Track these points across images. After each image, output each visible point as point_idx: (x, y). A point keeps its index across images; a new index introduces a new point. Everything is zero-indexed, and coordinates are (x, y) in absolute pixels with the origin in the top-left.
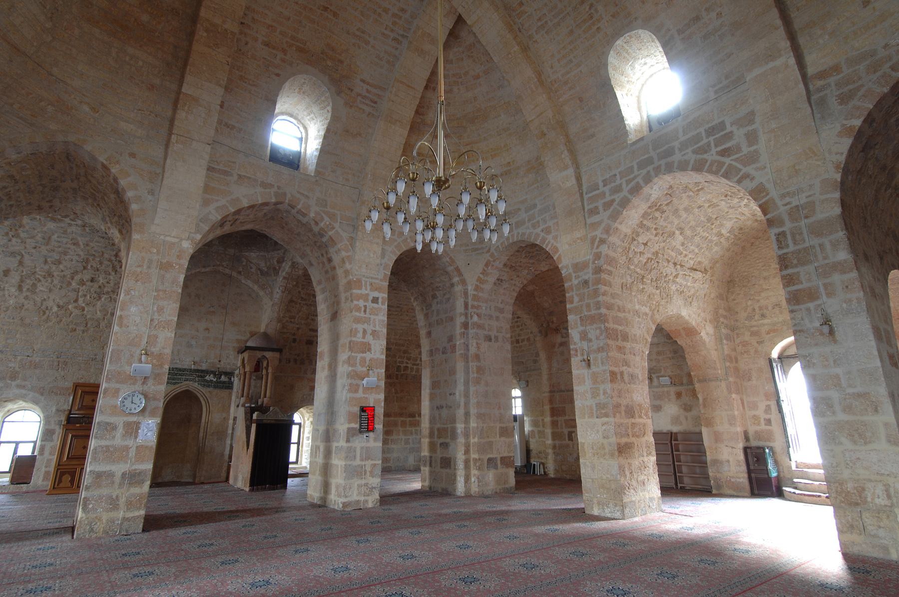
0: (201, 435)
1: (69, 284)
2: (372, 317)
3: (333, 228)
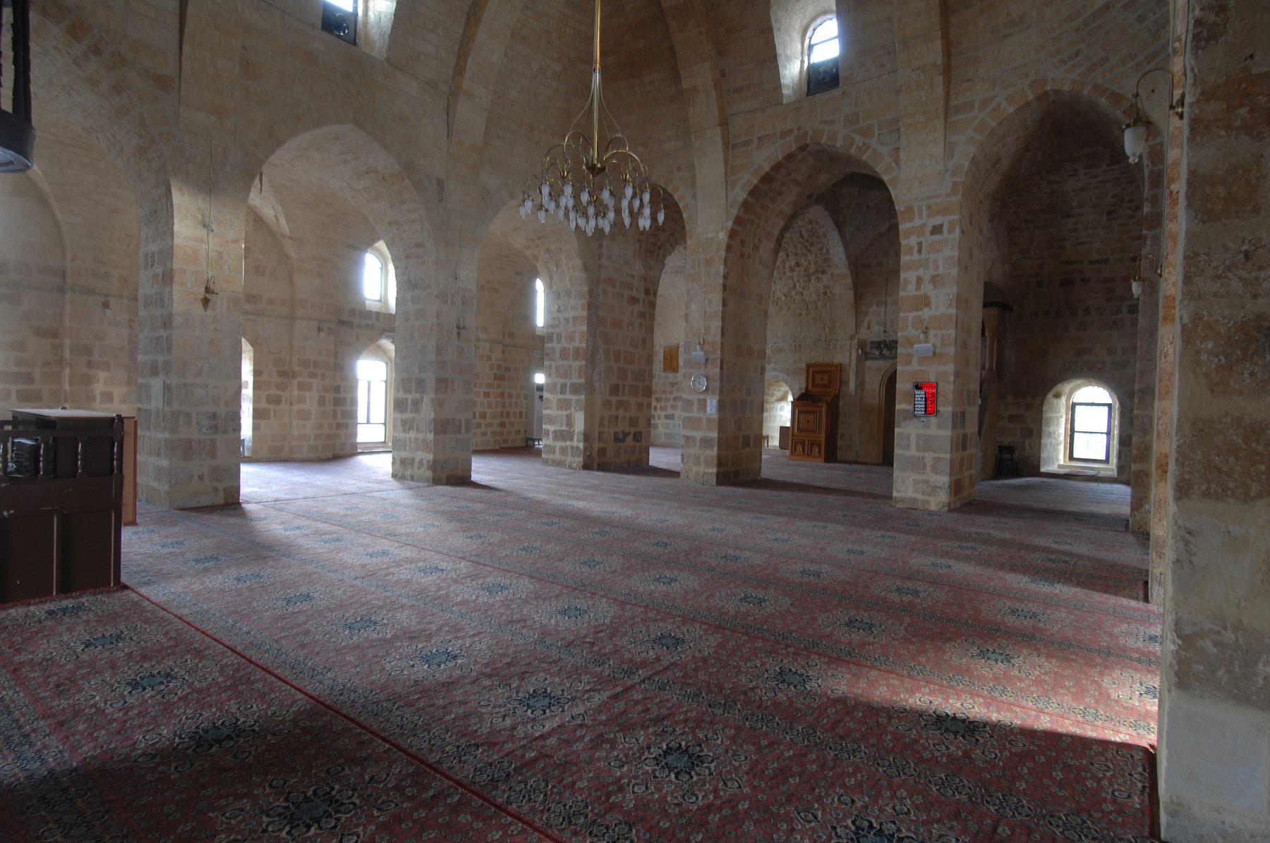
1: (784, 273)
2: (932, 256)
3: (868, 148)
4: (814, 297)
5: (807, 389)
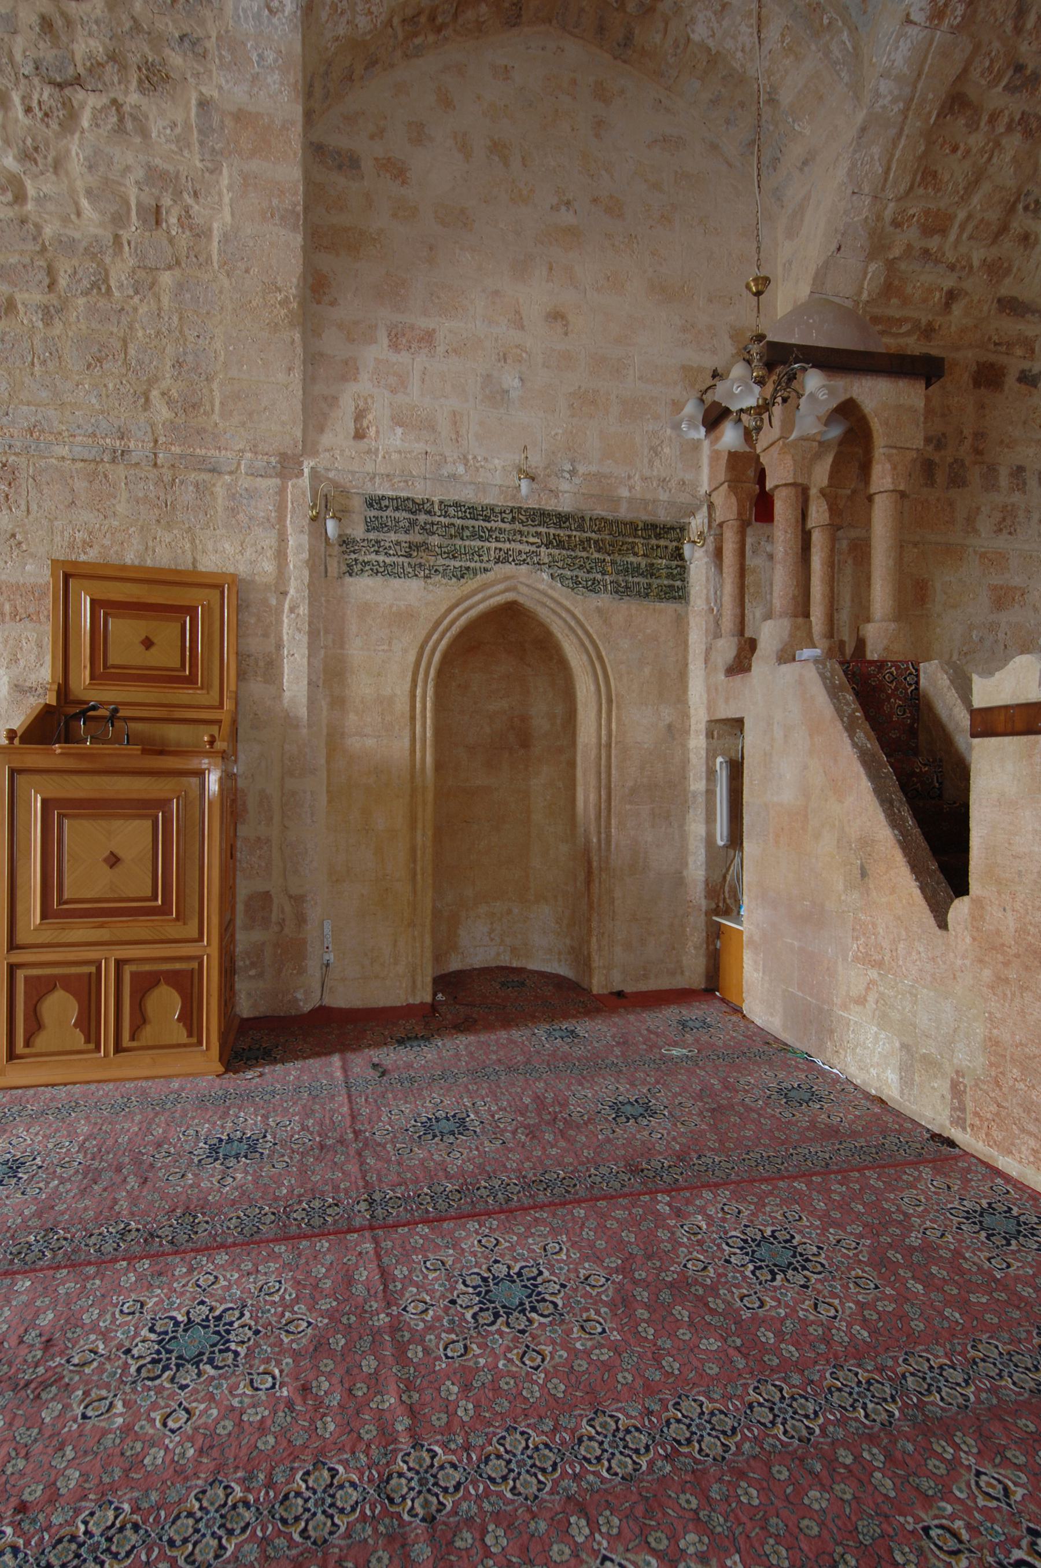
0: (586, 796)
4: (92, 220)
5: (63, 690)
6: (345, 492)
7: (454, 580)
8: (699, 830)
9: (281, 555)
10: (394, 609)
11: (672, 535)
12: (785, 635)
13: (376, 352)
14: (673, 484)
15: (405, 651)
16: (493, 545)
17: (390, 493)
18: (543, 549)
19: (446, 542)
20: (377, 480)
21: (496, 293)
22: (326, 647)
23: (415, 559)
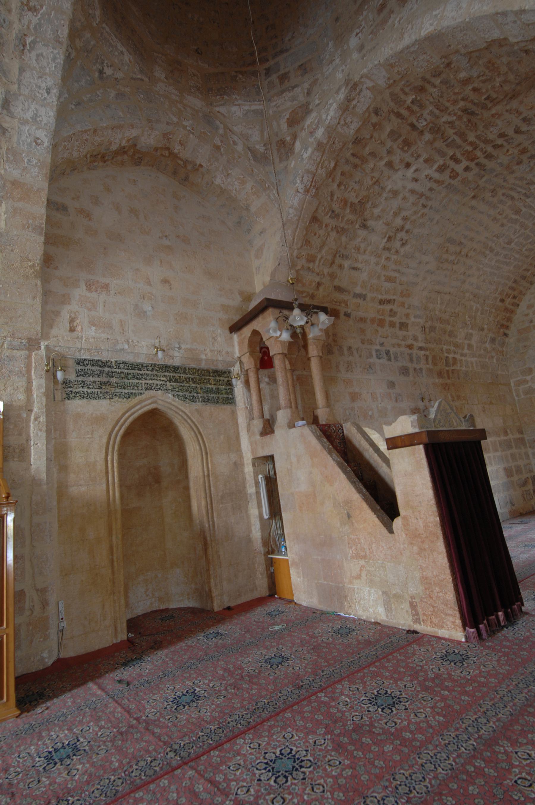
0: (198, 504)
6: (64, 357)
7: (125, 399)
8: (257, 511)
9: (29, 390)
10: (94, 415)
11: (225, 375)
12: (289, 415)
13: (79, 292)
14: (224, 353)
15: (101, 437)
16: (144, 382)
17: (89, 358)
18: (168, 383)
19: (120, 381)
20: (82, 352)
21: (137, 270)
22: (55, 438)
23: (104, 390)
